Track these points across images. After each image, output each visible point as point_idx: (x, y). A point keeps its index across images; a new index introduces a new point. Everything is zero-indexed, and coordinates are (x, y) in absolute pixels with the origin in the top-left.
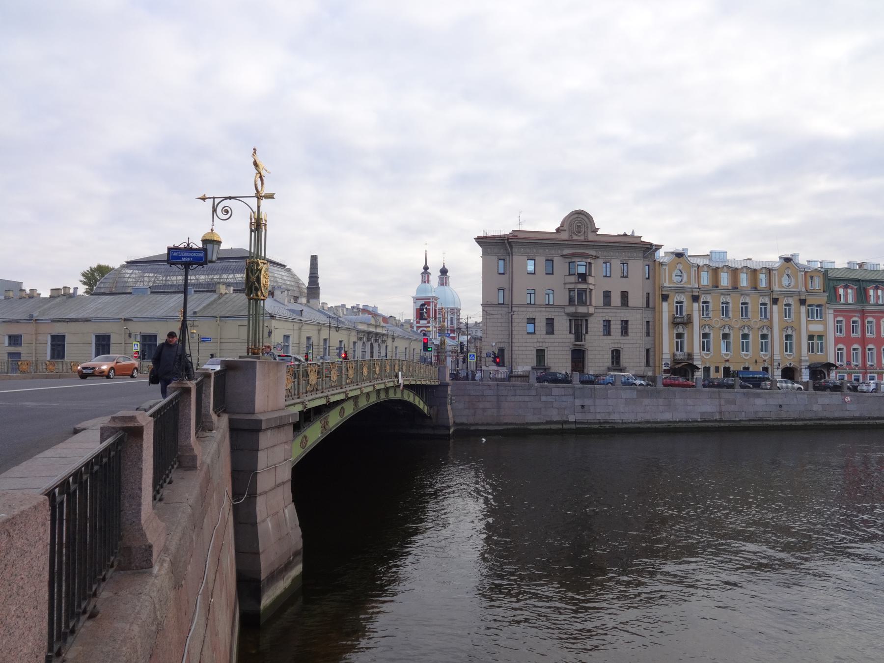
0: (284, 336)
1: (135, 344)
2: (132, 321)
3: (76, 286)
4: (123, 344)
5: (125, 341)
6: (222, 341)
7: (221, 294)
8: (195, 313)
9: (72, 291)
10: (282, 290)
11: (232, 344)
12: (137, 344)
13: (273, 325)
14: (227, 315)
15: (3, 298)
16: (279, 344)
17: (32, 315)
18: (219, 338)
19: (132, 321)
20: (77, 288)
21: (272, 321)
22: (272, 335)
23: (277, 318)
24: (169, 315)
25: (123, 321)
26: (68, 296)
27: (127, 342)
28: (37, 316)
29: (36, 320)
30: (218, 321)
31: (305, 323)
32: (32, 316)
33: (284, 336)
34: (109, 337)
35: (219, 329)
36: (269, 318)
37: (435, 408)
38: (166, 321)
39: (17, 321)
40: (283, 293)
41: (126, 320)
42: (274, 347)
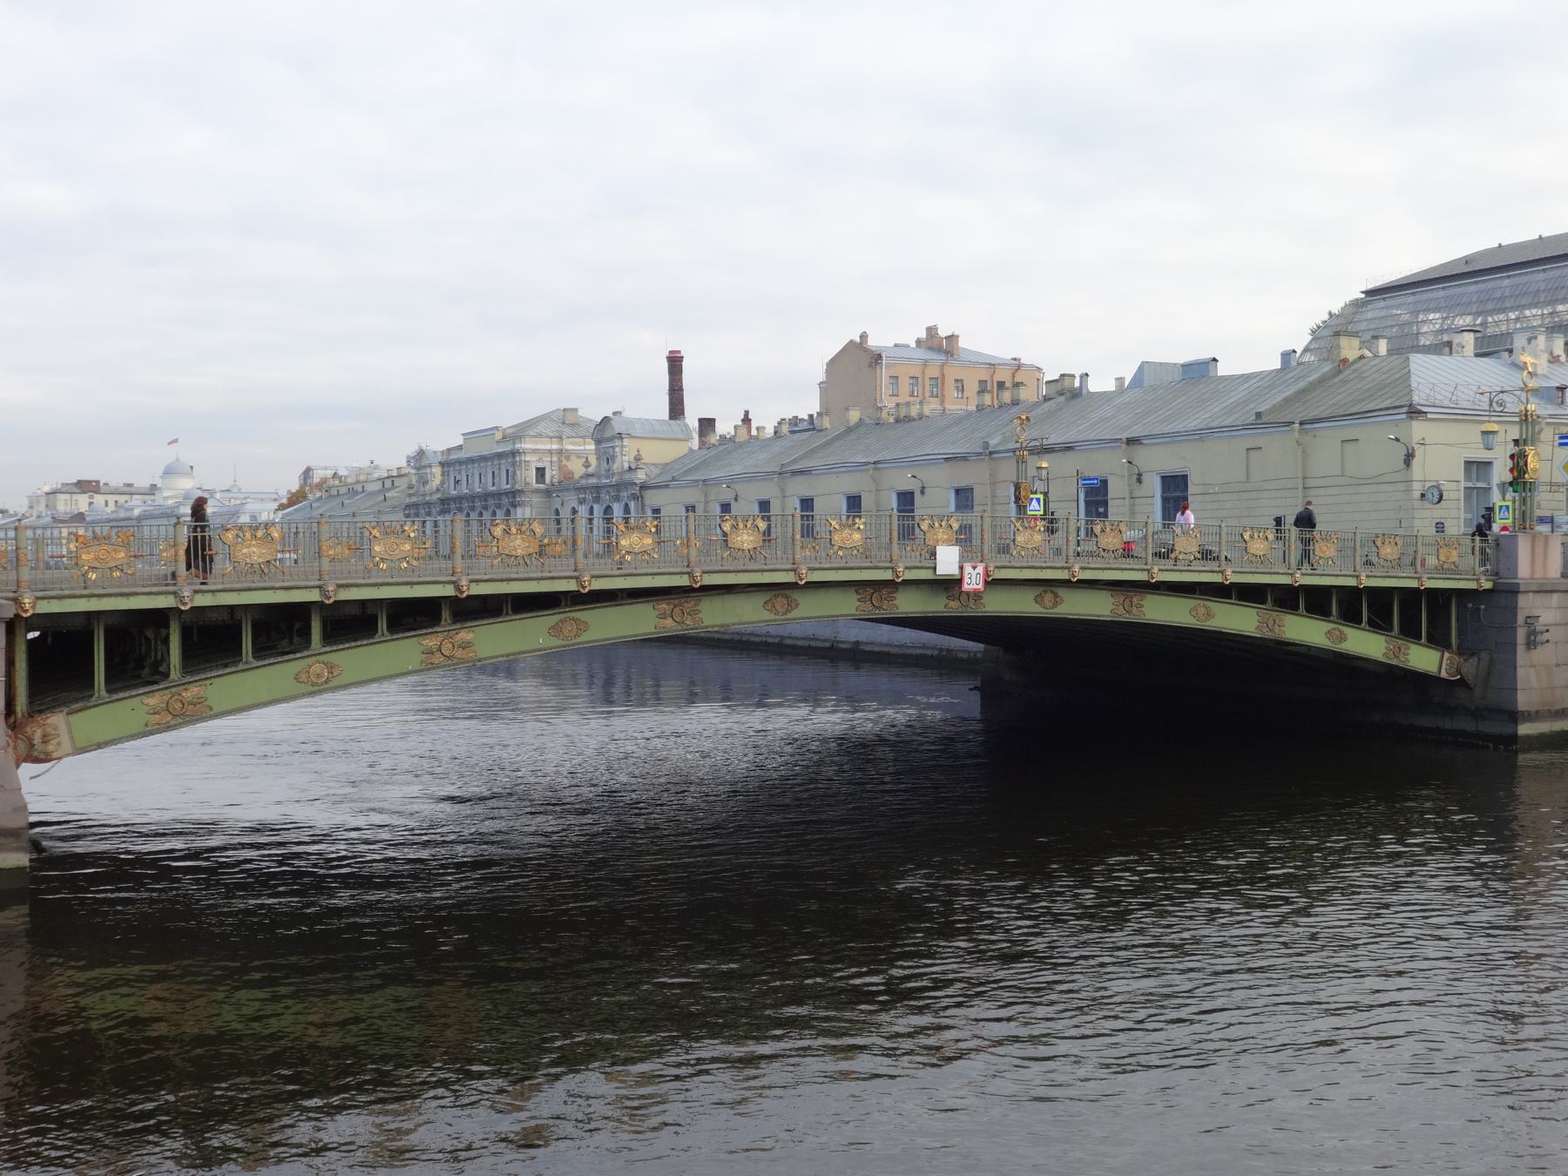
0: (1466, 462)
1: (1032, 499)
2: (1141, 444)
3: (1085, 372)
4: (1127, 501)
5: (1131, 493)
6: (1310, 483)
7: (1345, 361)
8: (1259, 415)
9: (1077, 384)
10: (1528, 335)
11: (1331, 491)
12: (1038, 500)
13: (1416, 437)
14: (1323, 415)
15: (975, 408)
16: (1437, 487)
17: (987, 443)
18: (1300, 475)
19: (1141, 444)
20: (1087, 375)
21: (1414, 423)
22: (1415, 462)
23: (1429, 416)
24: (1209, 426)
25: (1124, 446)
26: (1069, 395)
27: (1136, 494)
28: (998, 444)
29: (991, 453)
30: (1296, 434)
31: (1548, 424)
32: (986, 445)
33: (1469, 464)
34: (1185, 477)
35: (1300, 454)
36: (1404, 416)
37: (1485, 656)
38: (1201, 439)
39: (964, 458)
40: (1533, 341)
41: (1131, 441)
42: (1423, 495)
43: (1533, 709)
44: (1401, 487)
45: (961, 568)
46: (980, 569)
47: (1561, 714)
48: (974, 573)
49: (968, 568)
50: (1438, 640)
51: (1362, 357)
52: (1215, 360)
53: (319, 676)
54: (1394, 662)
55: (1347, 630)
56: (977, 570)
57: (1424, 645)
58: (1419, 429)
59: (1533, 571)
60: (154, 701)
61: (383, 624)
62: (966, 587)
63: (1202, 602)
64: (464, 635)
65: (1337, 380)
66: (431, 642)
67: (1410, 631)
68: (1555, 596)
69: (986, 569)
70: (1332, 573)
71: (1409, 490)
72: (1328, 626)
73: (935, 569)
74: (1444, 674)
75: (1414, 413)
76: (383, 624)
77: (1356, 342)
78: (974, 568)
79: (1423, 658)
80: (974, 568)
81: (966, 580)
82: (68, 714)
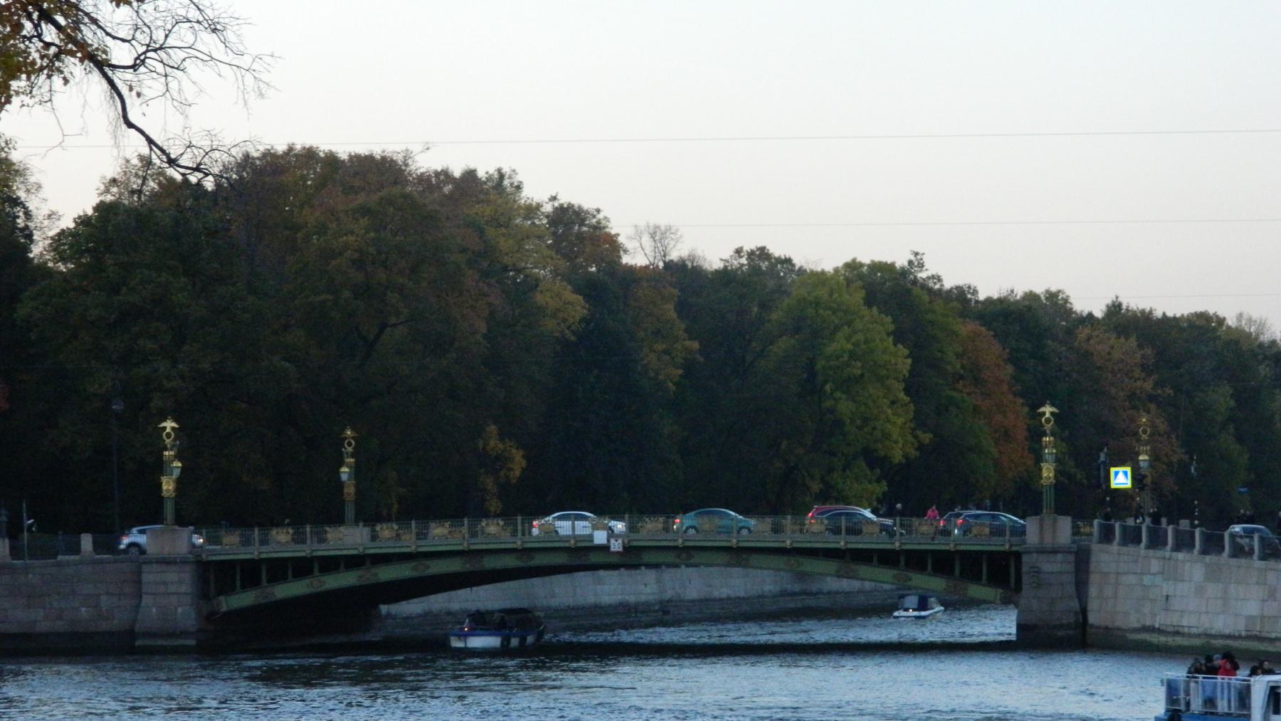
45: (608, 541)
48: (616, 543)
49: (613, 541)
56: (618, 542)
57: (983, 585)
59: (1042, 538)
60: (254, 592)
62: (612, 550)
64: (373, 571)
66: (360, 573)
69: (623, 543)
72: (895, 572)
76: (342, 566)
78: (616, 541)
80: (616, 541)
81: (612, 546)
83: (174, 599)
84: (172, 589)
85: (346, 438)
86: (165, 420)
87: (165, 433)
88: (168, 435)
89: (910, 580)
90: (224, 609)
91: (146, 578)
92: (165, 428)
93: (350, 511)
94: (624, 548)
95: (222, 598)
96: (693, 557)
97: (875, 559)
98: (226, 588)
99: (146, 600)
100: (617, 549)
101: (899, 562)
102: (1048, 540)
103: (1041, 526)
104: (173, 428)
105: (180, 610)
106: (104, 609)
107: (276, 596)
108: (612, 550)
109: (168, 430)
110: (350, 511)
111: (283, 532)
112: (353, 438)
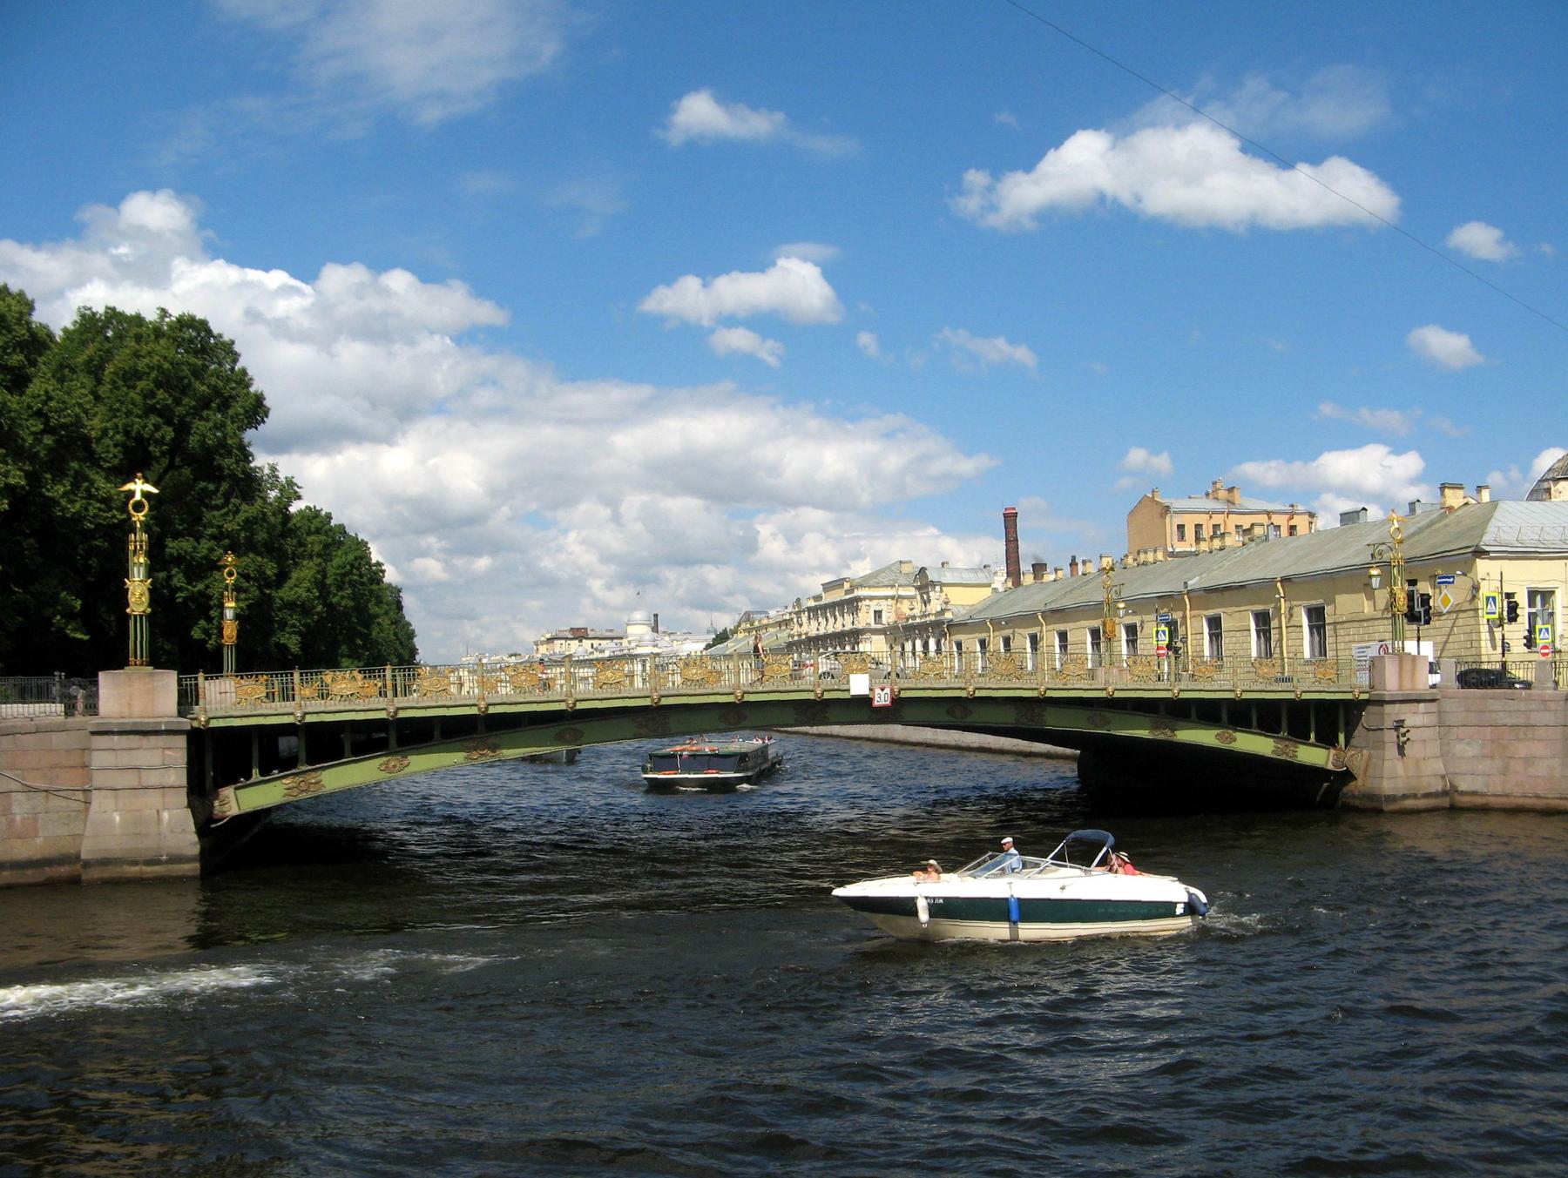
7: (1450, 509)
43: (1400, 794)
44: (1471, 613)
45: (871, 690)
46: (887, 690)
47: (1566, 798)
48: (883, 693)
49: (878, 691)
50: (1327, 740)
51: (1466, 504)
52: (1364, 509)
53: (394, 766)
54: (1283, 757)
55: (1238, 735)
56: (885, 691)
58: (1482, 566)
61: (437, 733)
62: (876, 703)
63: (1098, 713)
65: (1440, 525)
67: (1300, 735)
68: (1422, 705)
69: (892, 690)
70: (1195, 688)
71: (1477, 616)
73: (848, 690)
74: (1330, 767)
75: (1480, 553)
77: (1460, 493)
78: (883, 690)
79: (1311, 755)
80: (883, 690)
81: (877, 699)
82: (236, 789)
83: (152, 800)
84: (152, 778)
85: (226, 566)
86: (131, 479)
87: (131, 502)
88: (138, 507)
89: (1235, 740)
90: (233, 810)
91: (99, 759)
92: (131, 494)
93: (229, 659)
94: (893, 700)
95: (228, 792)
96: (971, 712)
97: (1193, 713)
98: (235, 773)
99: (100, 801)
100: (882, 703)
101: (1190, 716)
102: (1408, 690)
103: (1401, 668)
104: (146, 495)
105: (166, 815)
106: (18, 818)
107: (323, 786)
108: (876, 703)
109: (138, 497)
110: (229, 659)
111: (344, 678)
112: (235, 566)
